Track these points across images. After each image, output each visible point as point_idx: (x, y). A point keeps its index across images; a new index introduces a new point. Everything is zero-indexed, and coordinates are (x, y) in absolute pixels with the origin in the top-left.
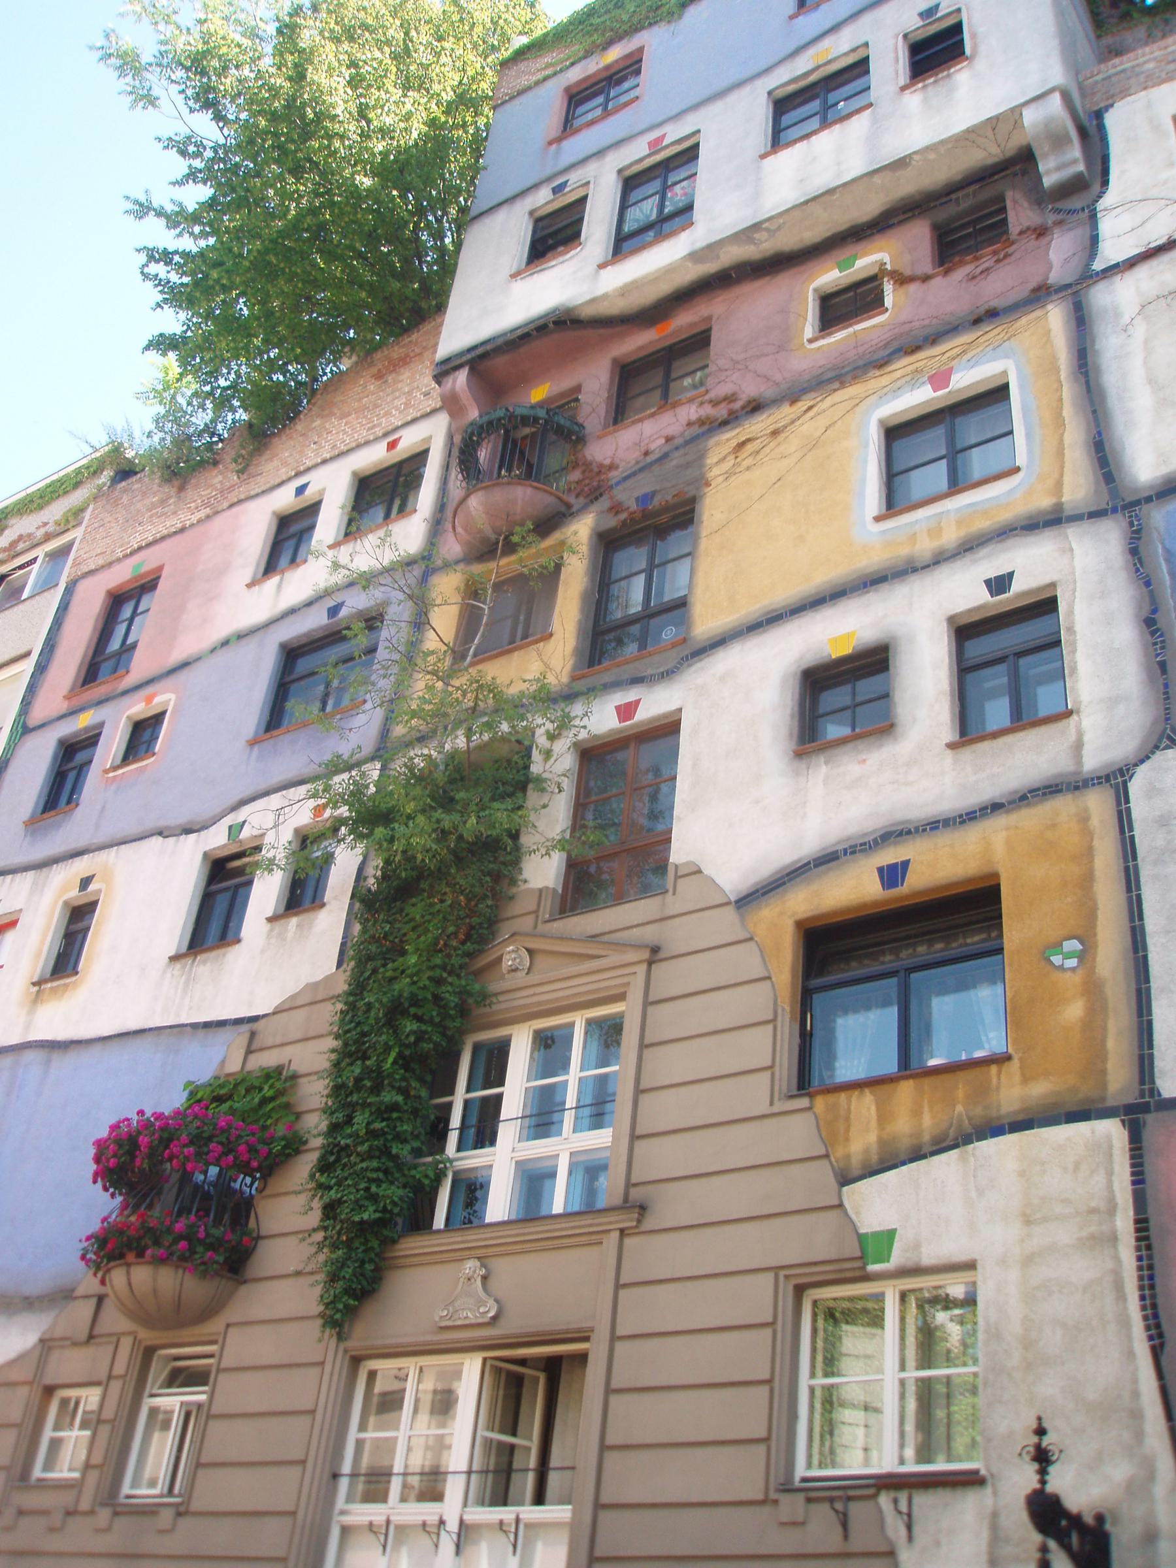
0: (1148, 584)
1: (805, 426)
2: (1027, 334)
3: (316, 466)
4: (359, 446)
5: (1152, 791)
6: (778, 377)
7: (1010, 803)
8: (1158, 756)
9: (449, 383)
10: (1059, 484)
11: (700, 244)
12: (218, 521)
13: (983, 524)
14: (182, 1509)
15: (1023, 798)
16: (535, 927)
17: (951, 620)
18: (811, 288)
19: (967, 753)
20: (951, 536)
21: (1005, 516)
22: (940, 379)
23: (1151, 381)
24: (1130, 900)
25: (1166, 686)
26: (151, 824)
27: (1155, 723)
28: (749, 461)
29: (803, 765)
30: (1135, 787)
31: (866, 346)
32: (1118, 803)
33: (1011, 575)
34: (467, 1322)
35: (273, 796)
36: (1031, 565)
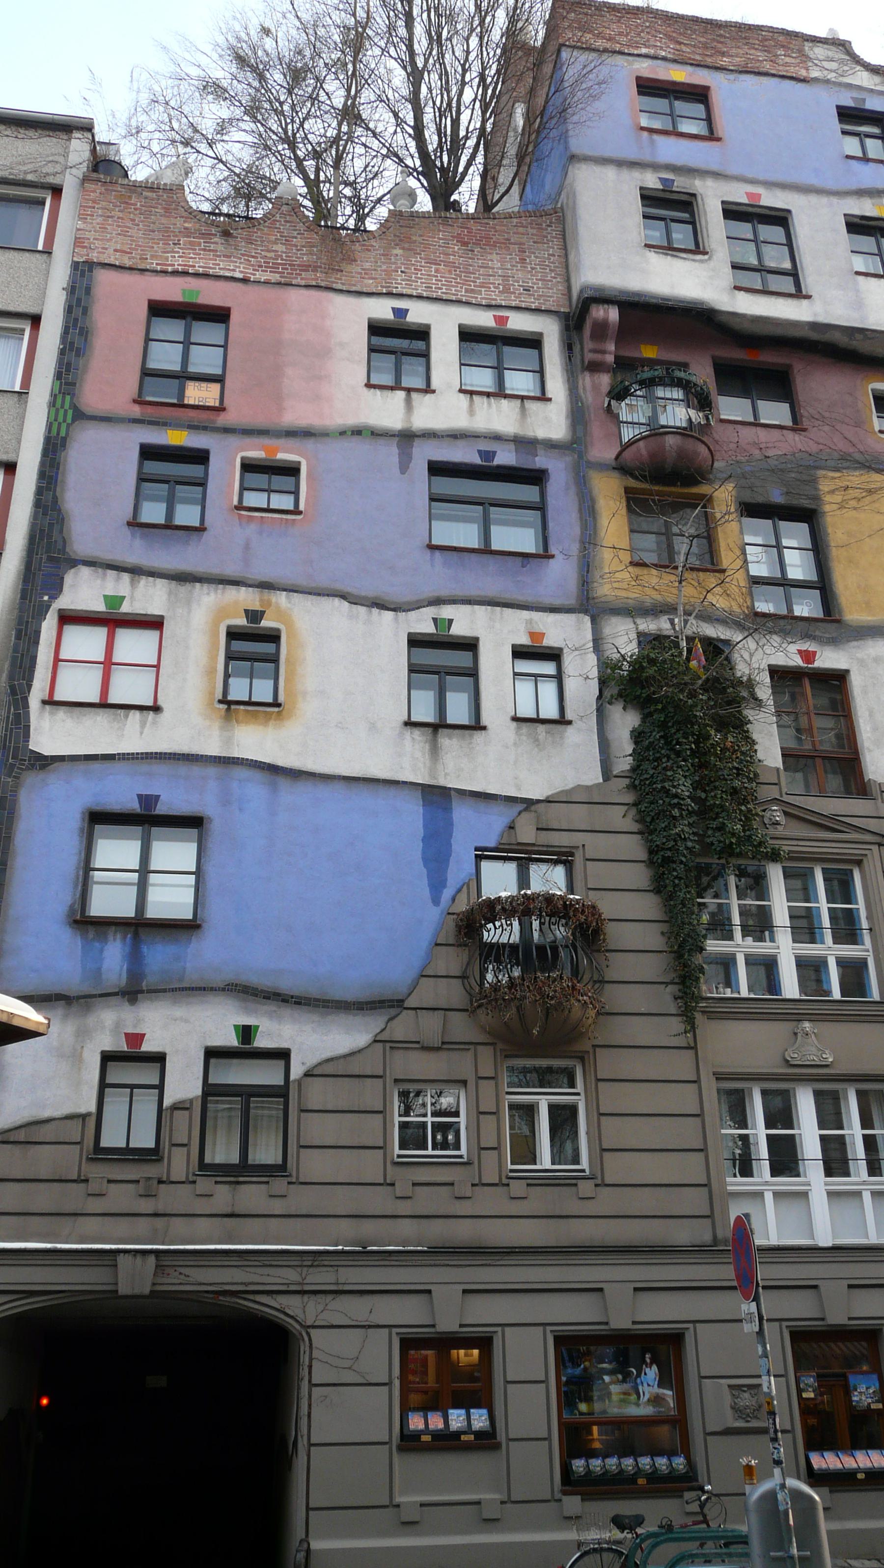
3: (410, 296)
4: (459, 302)
9: (598, 312)
11: (822, 319)
12: (295, 296)
14: (599, 1182)
16: (781, 796)
26: (323, 581)
28: (853, 503)
34: (813, 1063)
35: (476, 607)
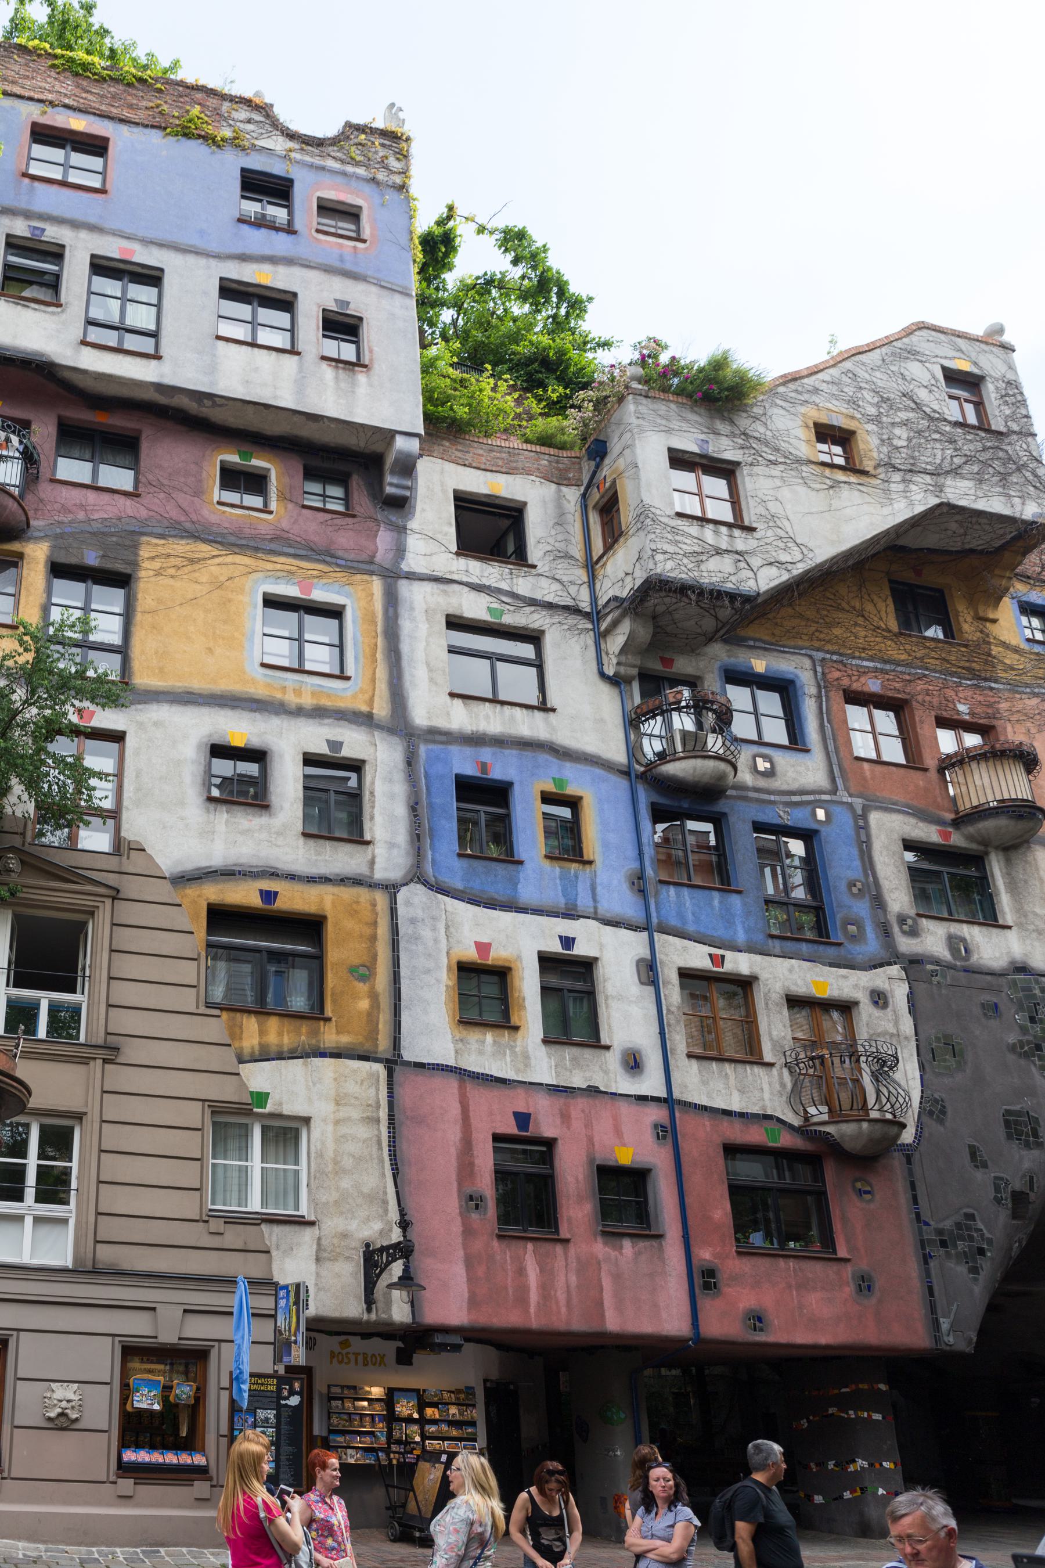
0: (414, 786)
1: (213, 568)
2: (360, 588)
5: (408, 903)
6: (194, 517)
7: (336, 880)
8: (412, 885)
10: (371, 702)
13: (325, 702)
15: (342, 880)
17: (305, 754)
18: (220, 457)
19: (311, 843)
20: (307, 701)
21: (341, 705)
22: (307, 589)
23: (428, 664)
24: (394, 956)
25: (419, 849)
27: (412, 866)
29: (208, 804)
30: (400, 897)
31: (257, 532)
32: (391, 903)
33: (342, 743)
36: (354, 742)
